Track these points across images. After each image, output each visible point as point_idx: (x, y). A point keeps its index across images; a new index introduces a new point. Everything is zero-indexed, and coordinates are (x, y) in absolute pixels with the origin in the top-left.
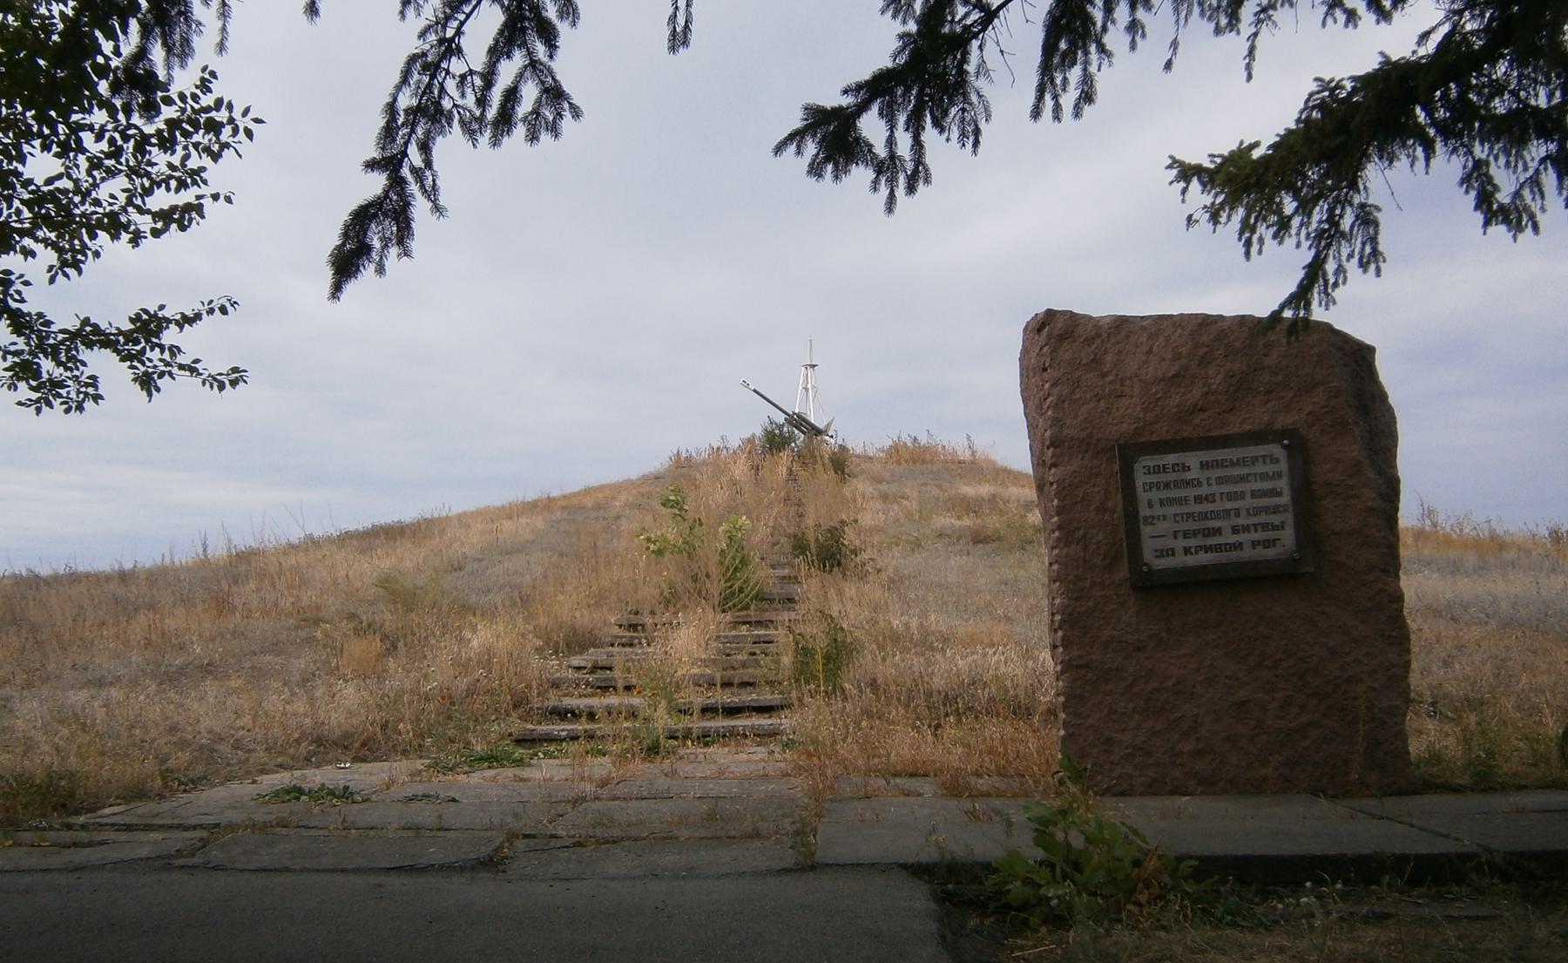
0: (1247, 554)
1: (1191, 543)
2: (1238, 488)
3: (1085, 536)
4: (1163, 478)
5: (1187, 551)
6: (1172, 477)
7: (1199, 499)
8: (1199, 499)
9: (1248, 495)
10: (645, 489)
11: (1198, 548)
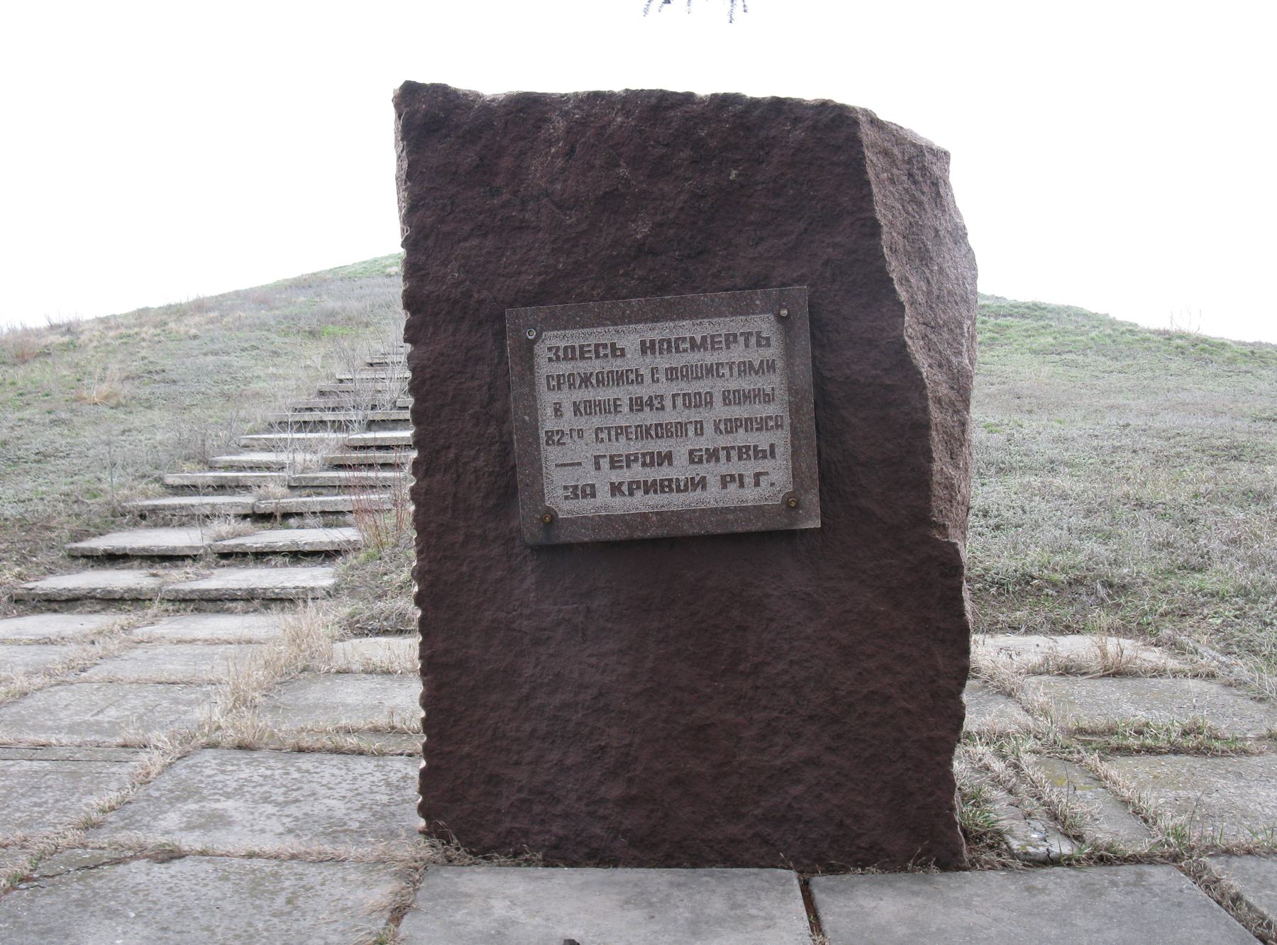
0: (712, 496)
1: (624, 476)
2: (703, 386)
3: (456, 460)
4: (583, 367)
5: (615, 489)
6: (595, 366)
7: (637, 405)
8: (637, 405)
9: (718, 399)
10: (120, 320)
11: (633, 487)
